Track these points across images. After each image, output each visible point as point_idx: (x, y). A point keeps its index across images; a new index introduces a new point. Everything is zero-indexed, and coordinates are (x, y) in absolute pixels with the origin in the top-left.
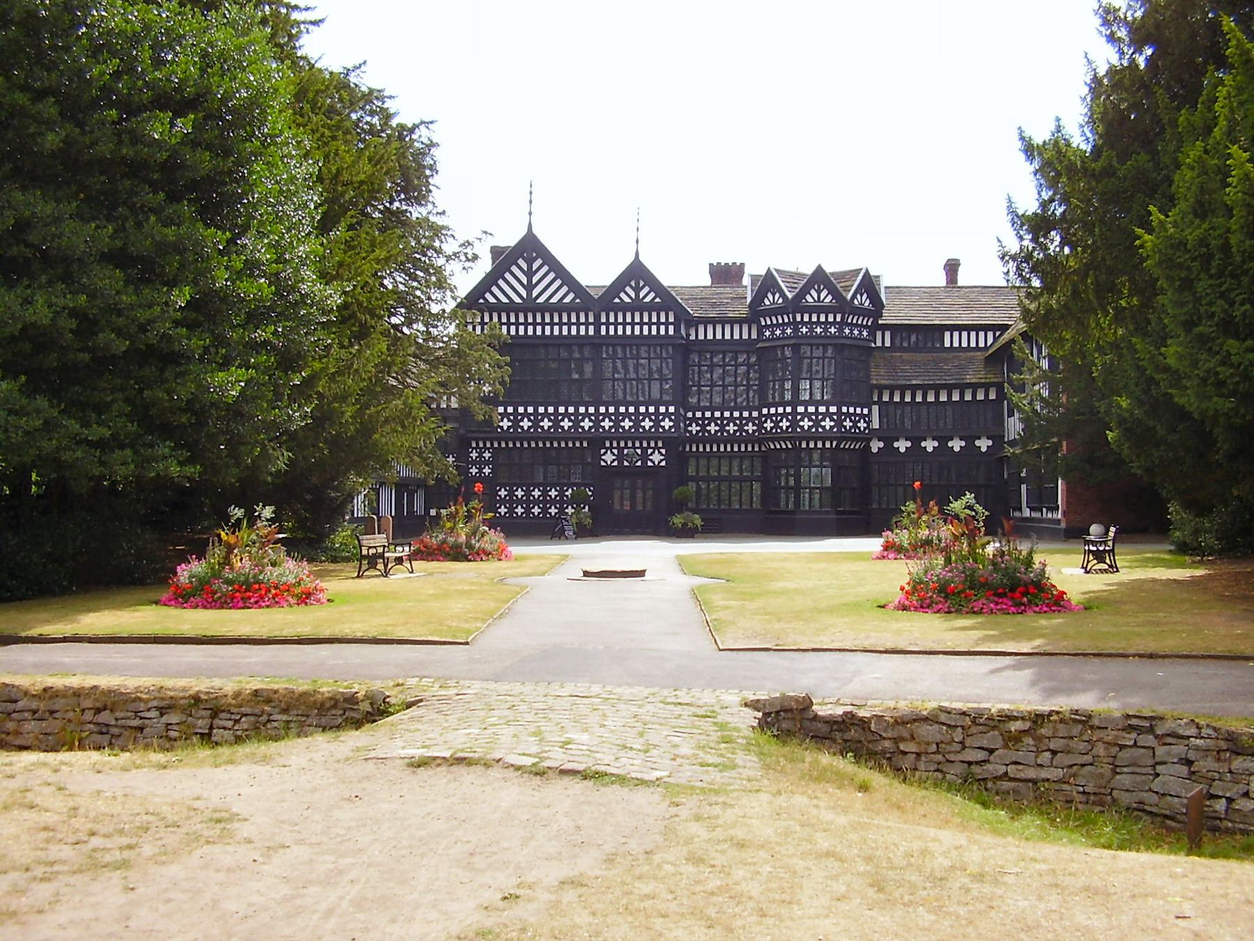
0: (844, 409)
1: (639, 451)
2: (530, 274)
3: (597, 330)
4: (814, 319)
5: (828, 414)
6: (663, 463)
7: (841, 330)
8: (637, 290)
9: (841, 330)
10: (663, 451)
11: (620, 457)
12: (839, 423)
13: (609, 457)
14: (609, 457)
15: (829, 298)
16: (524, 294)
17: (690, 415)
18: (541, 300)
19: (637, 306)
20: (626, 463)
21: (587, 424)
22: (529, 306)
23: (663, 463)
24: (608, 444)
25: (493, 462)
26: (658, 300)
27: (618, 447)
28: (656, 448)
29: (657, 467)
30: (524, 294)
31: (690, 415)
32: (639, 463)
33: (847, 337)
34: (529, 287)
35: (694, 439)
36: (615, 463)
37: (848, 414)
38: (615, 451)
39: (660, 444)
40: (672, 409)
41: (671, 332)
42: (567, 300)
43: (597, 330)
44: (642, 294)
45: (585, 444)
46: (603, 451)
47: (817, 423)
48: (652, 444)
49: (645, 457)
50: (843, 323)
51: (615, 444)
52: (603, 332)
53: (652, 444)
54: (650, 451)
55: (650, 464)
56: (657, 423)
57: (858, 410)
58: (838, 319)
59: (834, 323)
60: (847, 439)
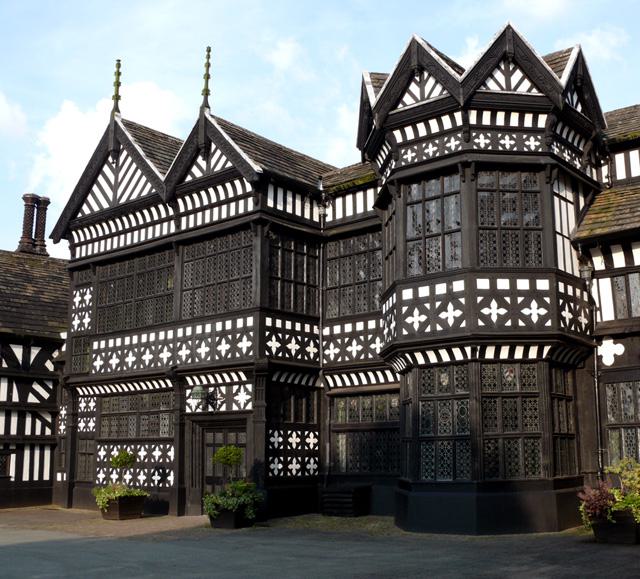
0: (483, 284)
1: (223, 389)
2: (116, 172)
3: (178, 226)
4: (422, 132)
5: (451, 296)
6: (249, 407)
7: (468, 139)
8: (207, 157)
9: (468, 139)
10: (249, 387)
12: (472, 310)
14: (193, 402)
15: (439, 88)
16: (110, 194)
17: (326, 331)
18: (123, 200)
19: (213, 180)
21: (165, 355)
22: (118, 211)
23: (249, 407)
25: (99, 415)
26: (229, 164)
28: (241, 383)
30: (110, 194)
31: (326, 331)
32: (223, 408)
33: (484, 151)
34: (114, 188)
35: (335, 369)
37: (493, 293)
39: (244, 378)
40: (250, 321)
41: (251, 208)
42: (145, 193)
43: (178, 226)
44: (213, 161)
47: (433, 316)
49: (230, 398)
50: (467, 130)
52: (184, 227)
55: (235, 408)
56: (234, 343)
57: (523, 284)
58: (459, 122)
59: (455, 130)
60: (498, 341)
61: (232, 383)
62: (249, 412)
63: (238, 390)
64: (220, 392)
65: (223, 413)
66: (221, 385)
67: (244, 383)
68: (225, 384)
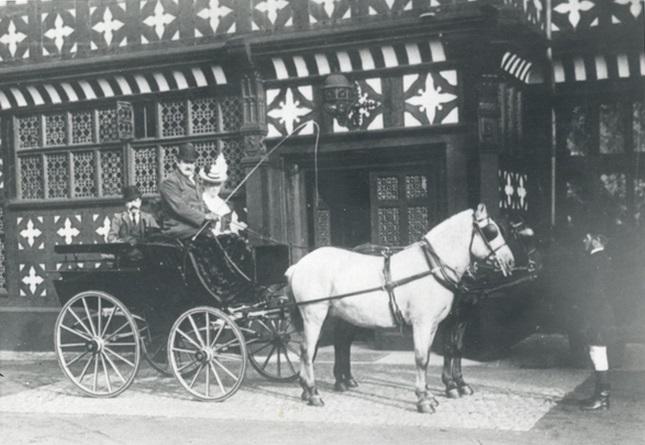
6: (452, 118)
10: (451, 77)
11: (321, 111)
13: (289, 113)
20: (338, 128)
23: (452, 118)
24: (282, 73)
27: (315, 80)
28: (427, 67)
29: (432, 132)
32: (378, 124)
36: (308, 129)
38: (307, 92)
39: (438, 55)
45: (220, 78)
46: (272, 94)
48: (414, 58)
49: (392, 102)
51: (302, 71)
53: (414, 58)
54: (409, 81)
55: (410, 121)
61: (404, 68)
62: (450, 128)
63: (420, 85)
64: (367, 89)
65: (377, 135)
66: (371, 74)
67: (436, 68)
68: (380, 72)
